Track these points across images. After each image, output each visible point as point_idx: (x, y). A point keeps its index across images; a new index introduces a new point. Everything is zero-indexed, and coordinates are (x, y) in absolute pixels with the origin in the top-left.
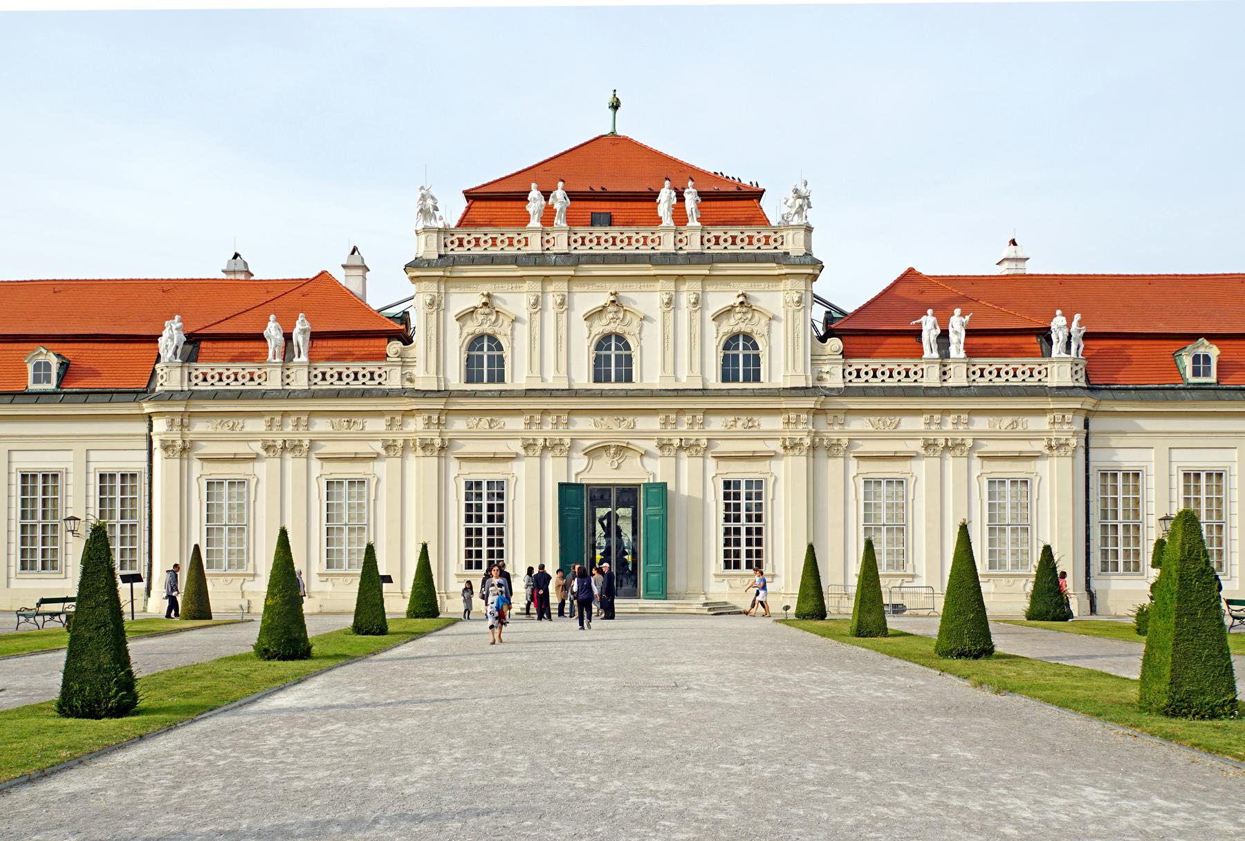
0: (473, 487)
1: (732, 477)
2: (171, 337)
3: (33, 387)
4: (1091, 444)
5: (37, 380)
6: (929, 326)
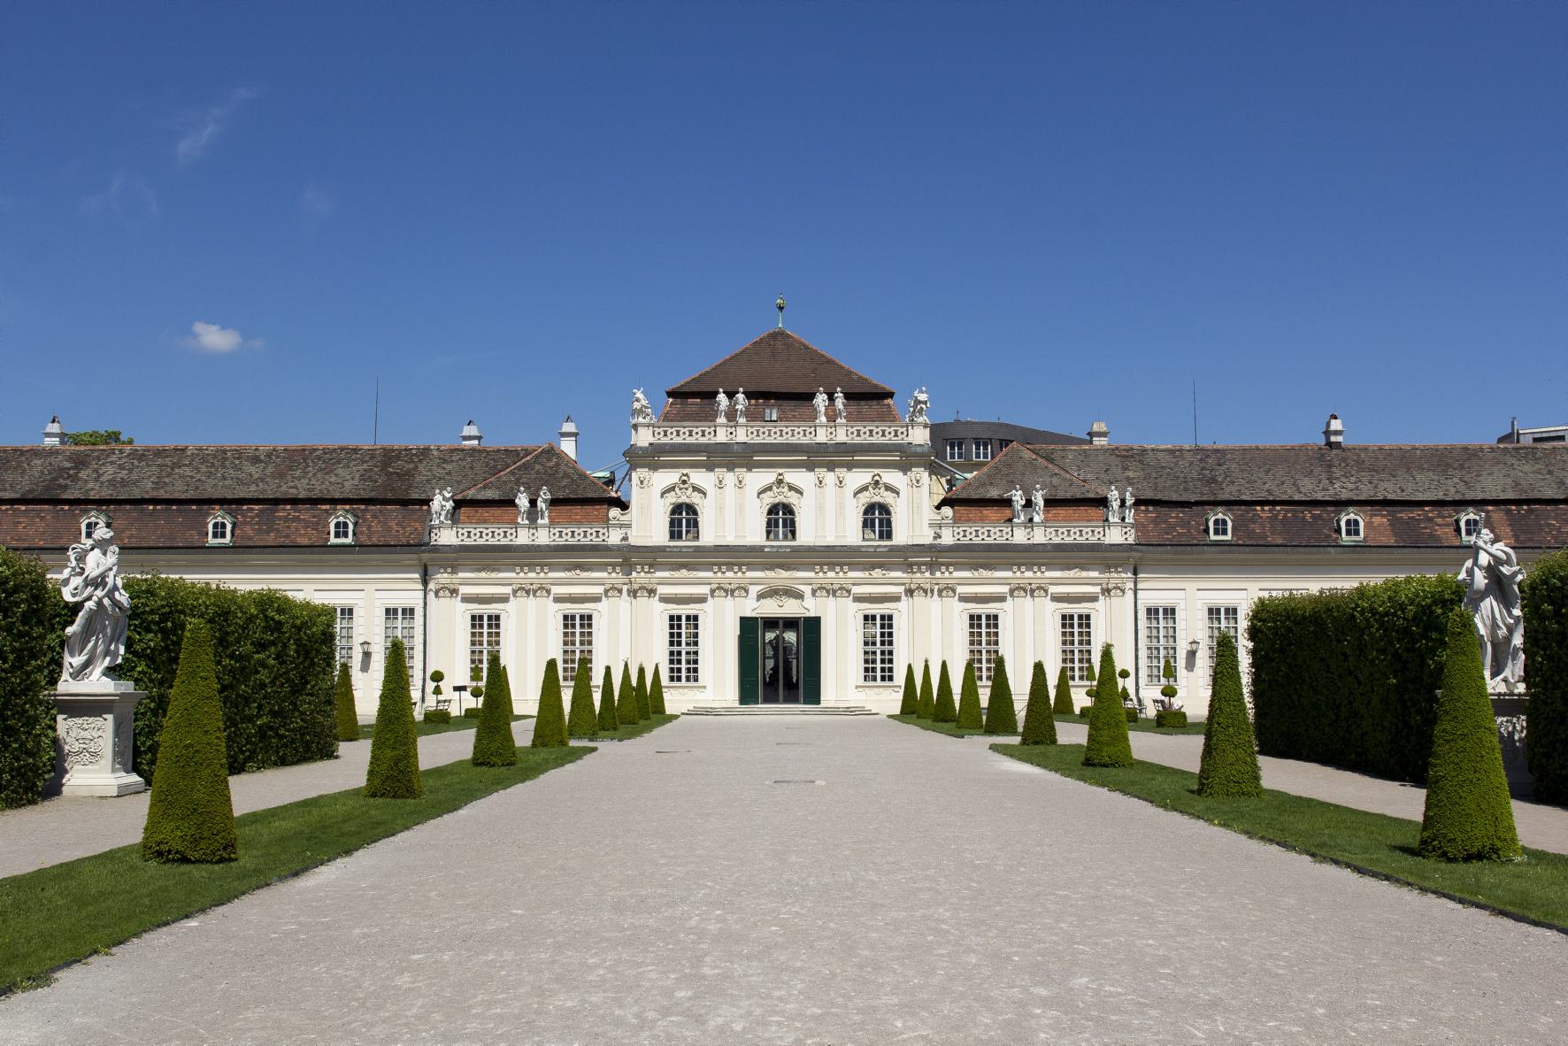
0: (674, 620)
2: (441, 503)
3: (333, 540)
5: (337, 535)
6: (1018, 498)
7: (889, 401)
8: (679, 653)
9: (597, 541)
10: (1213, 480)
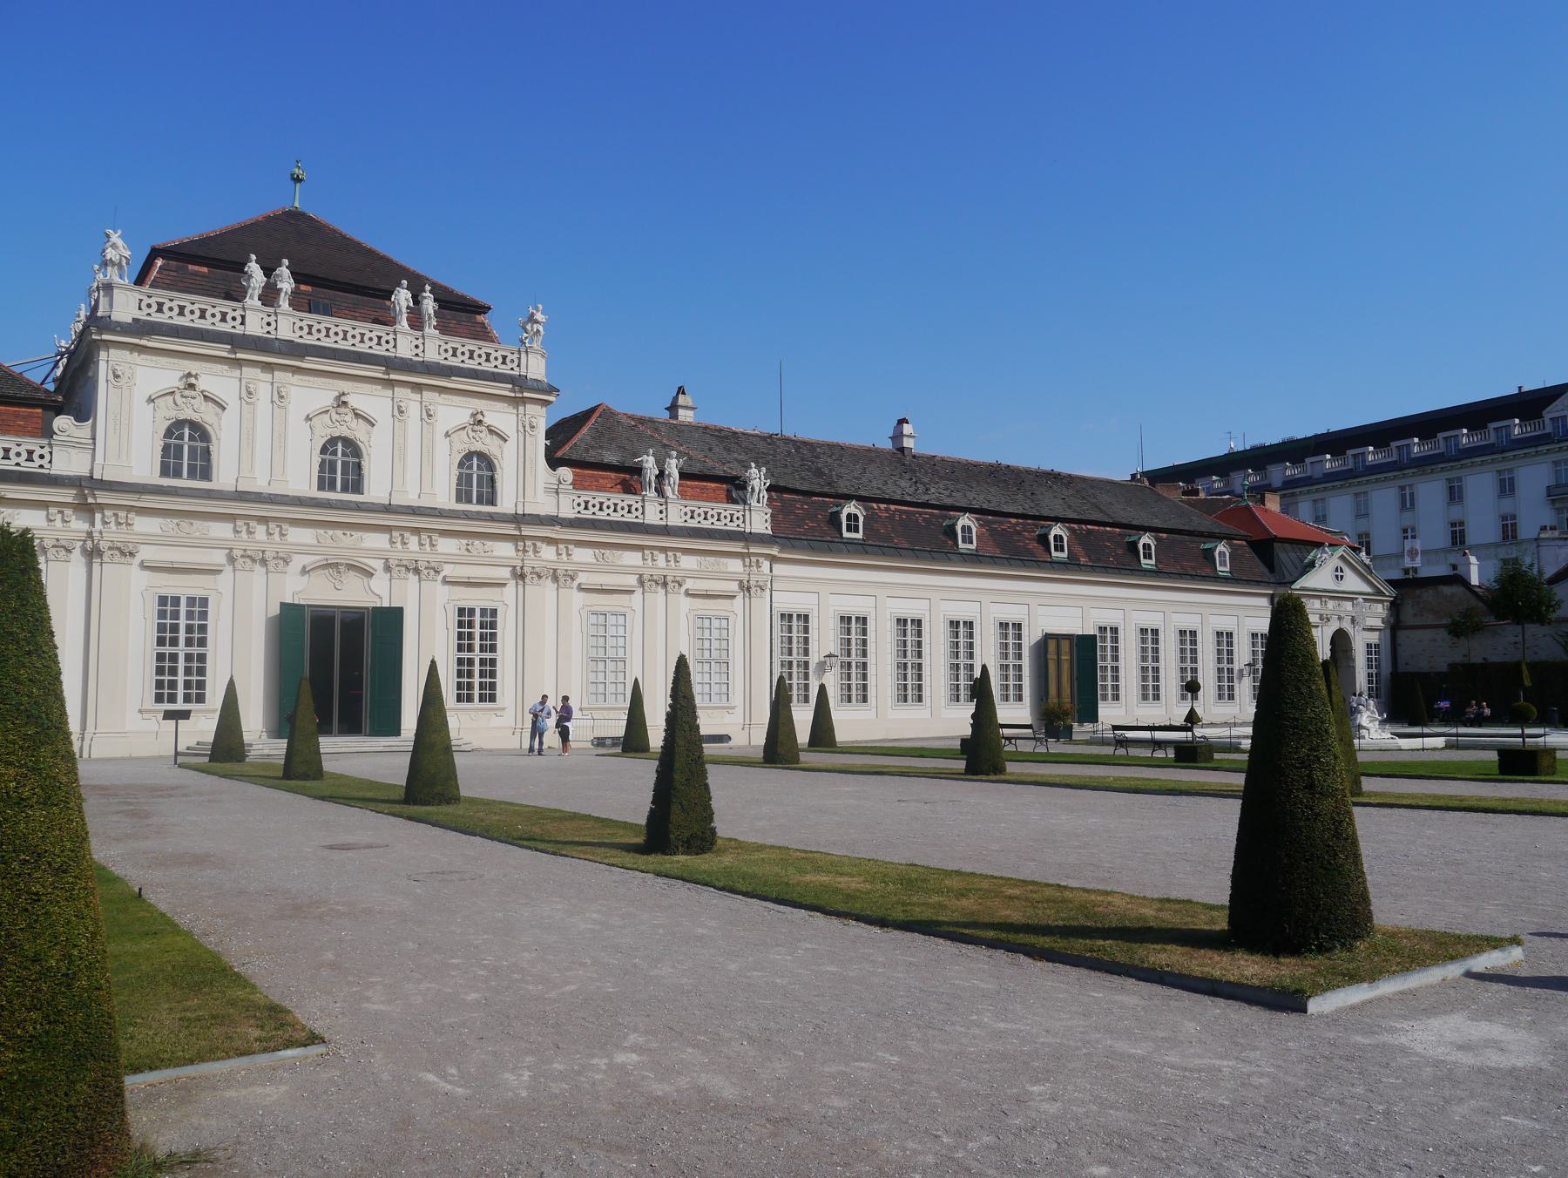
0: (167, 604)
1: (467, 604)
6: (649, 463)
7: (480, 318)
8: (174, 657)
9: (27, 467)
10: (819, 473)
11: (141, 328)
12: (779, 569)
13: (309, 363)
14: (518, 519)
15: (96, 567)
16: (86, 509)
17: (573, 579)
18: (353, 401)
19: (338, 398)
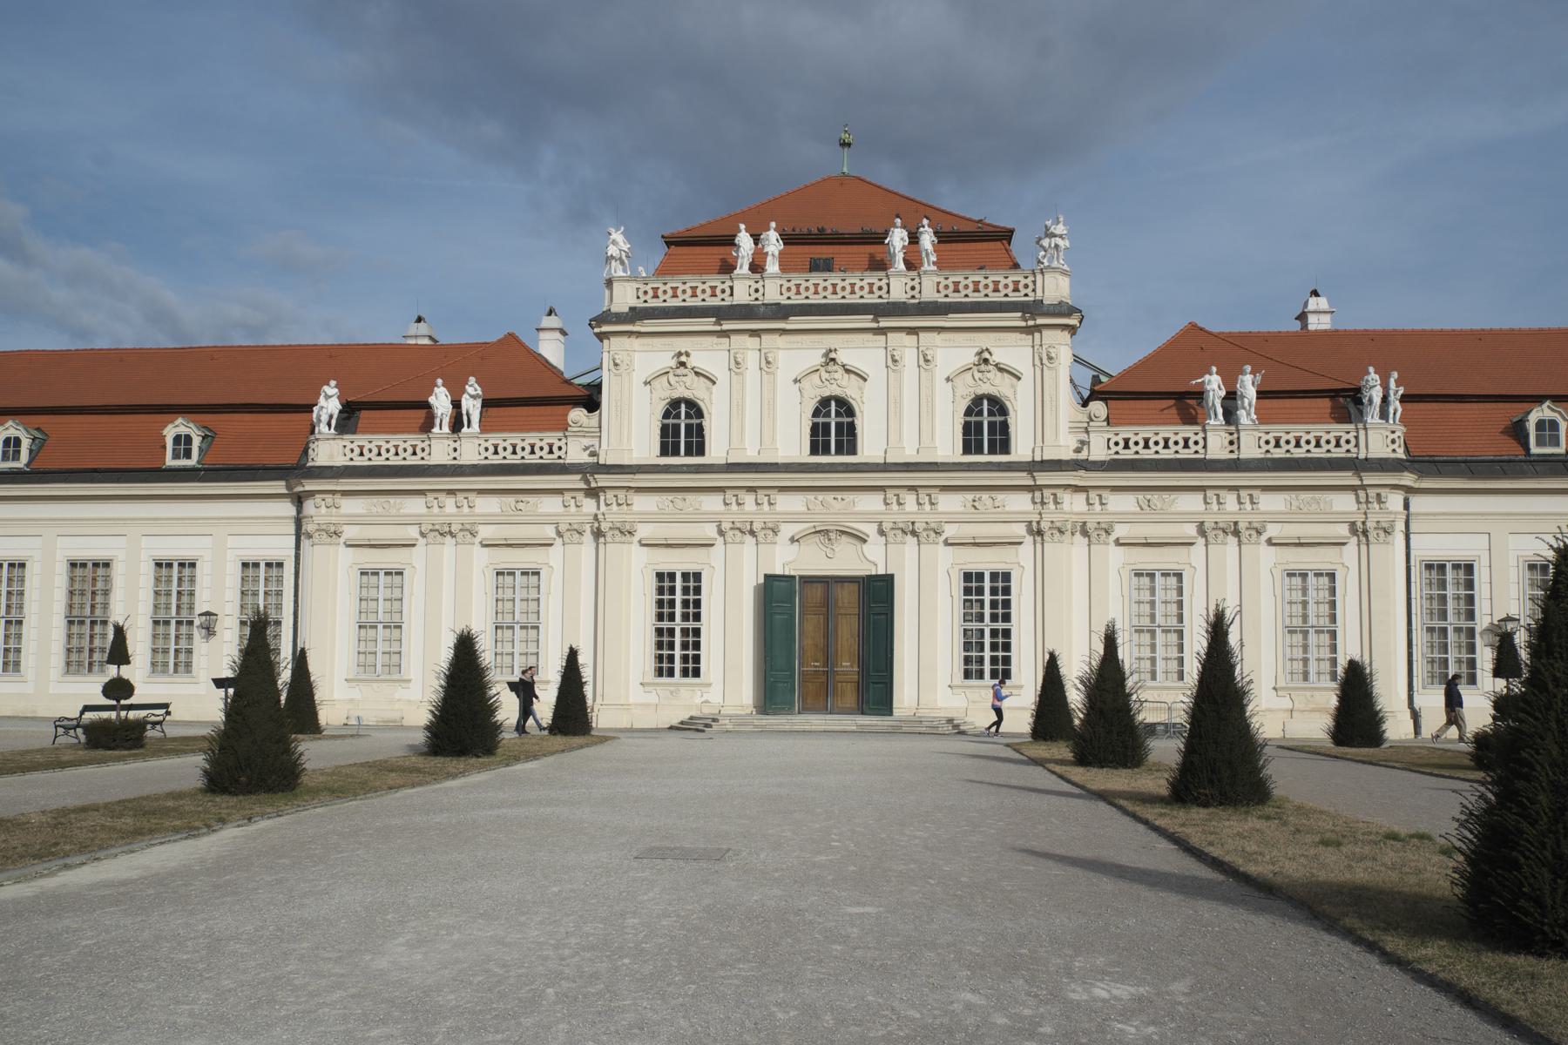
0: (664, 579)
3: (170, 462)
4: (1413, 528)
5: (176, 456)
6: (1214, 384)
9: (549, 459)
11: (636, 314)
12: (1418, 503)
13: (795, 323)
14: (1033, 467)
15: (601, 547)
16: (593, 493)
17: (1108, 533)
18: (842, 357)
19: (826, 355)
